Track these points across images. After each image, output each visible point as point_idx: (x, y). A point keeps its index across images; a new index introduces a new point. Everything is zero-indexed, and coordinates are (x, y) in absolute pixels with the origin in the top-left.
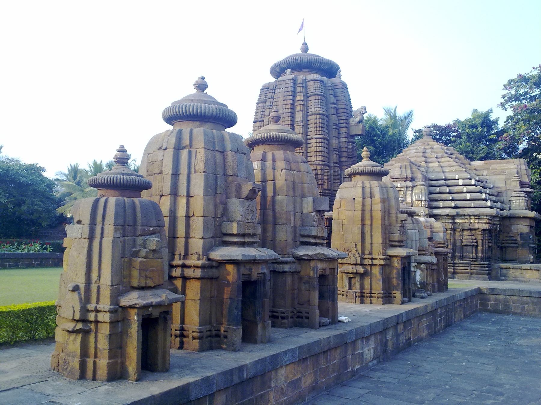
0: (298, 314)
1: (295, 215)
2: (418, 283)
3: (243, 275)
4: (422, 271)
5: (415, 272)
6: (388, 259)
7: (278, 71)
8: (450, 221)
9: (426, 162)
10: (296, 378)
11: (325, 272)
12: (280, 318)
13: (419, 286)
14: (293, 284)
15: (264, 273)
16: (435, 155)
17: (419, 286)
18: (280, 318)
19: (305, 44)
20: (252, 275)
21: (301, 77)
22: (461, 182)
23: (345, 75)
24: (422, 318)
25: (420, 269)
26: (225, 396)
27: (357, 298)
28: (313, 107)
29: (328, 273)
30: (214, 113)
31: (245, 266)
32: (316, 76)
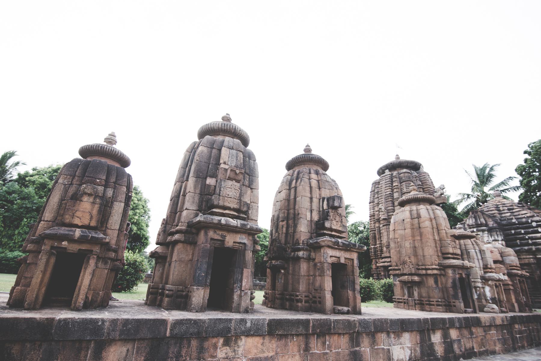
0: (314, 299)
1: (311, 212)
2: (489, 298)
3: (212, 239)
4: (491, 287)
5: (483, 288)
6: (443, 270)
7: (381, 172)
8: (531, 257)
9: (499, 214)
10: (265, 355)
11: (340, 260)
12: (295, 301)
13: (490, 301)
14: (308, 271)
15: (244, 244)
16: (506, 208)
17: (490, 301)
18: (295, 301)
19: (397, 155)
20: (226, 243)
21: (395, 173)
22: (534, 224)
23: (426, 168)
24: (490, 330)
25: (489, 285)
26: (124, 349)
27: (416, 306)
28: (405, 188)
29: (342, 261)
30: (220, 126)
31: (215, 232)
32: (405, 170)
